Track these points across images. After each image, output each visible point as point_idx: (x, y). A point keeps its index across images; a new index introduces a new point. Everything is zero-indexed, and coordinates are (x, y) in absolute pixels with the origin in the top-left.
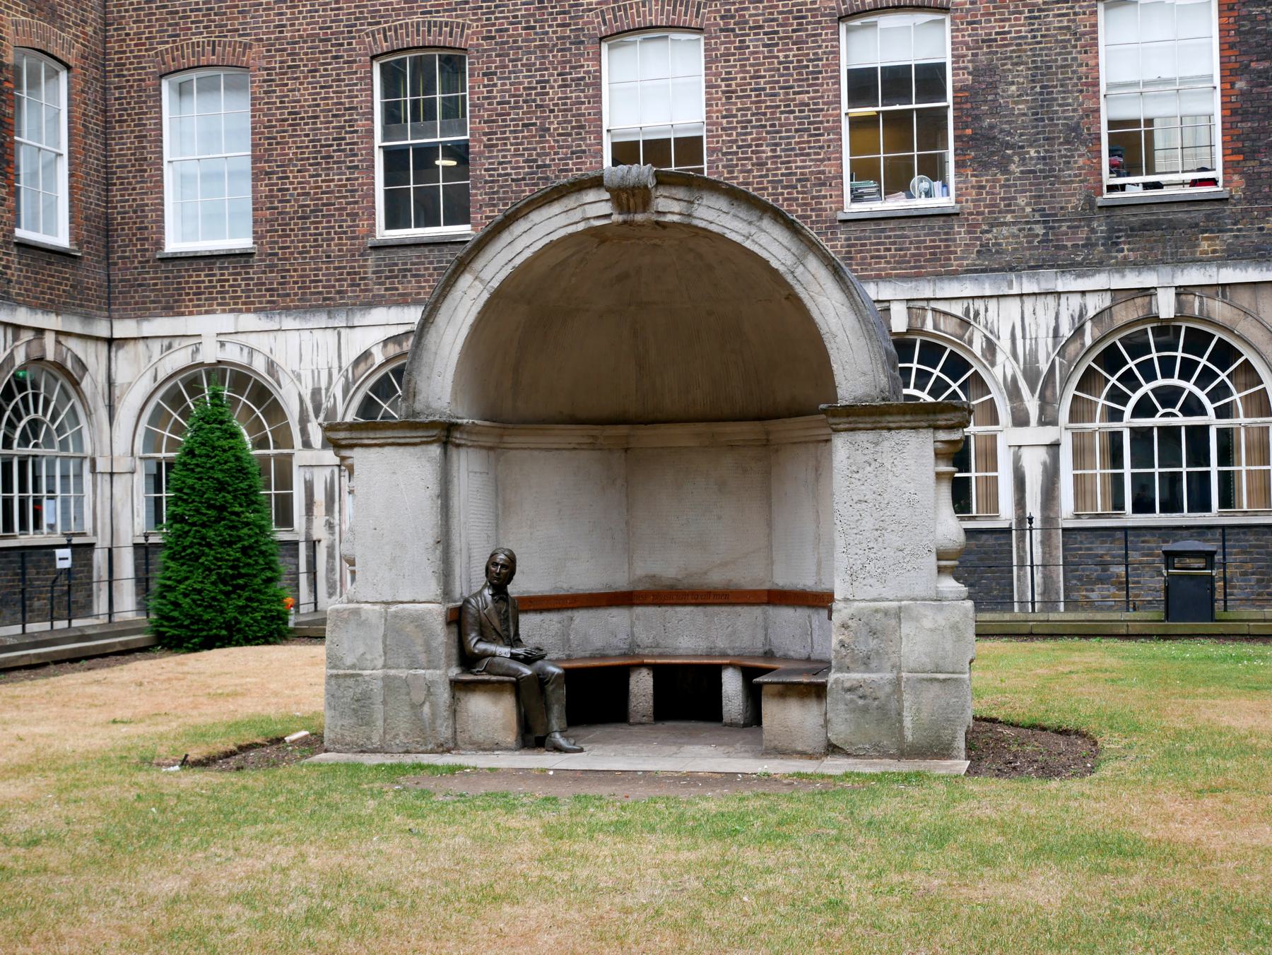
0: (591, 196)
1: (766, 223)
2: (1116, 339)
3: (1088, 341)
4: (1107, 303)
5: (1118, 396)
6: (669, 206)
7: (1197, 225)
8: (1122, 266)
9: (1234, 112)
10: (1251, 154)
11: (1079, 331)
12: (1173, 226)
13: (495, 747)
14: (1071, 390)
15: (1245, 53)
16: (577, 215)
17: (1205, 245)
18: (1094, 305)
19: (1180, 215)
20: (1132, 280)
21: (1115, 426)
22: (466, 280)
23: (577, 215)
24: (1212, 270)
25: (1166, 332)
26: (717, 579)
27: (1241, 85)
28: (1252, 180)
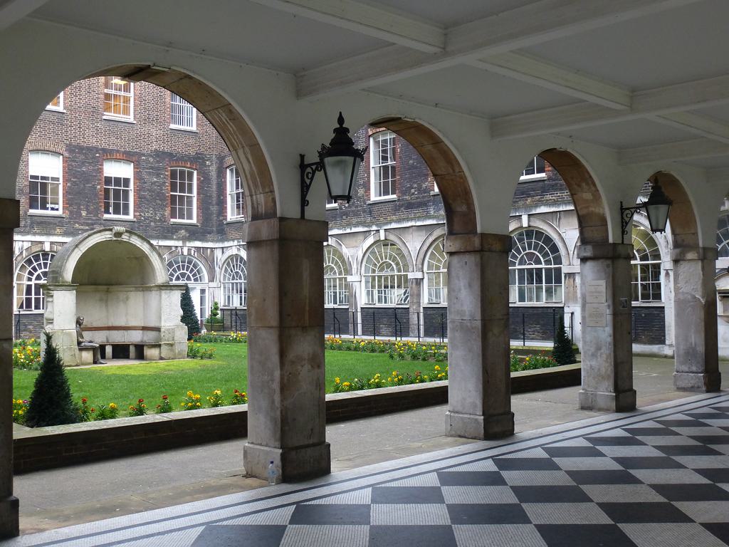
0: (107, 232)
1: (145, 243)
2: (31, 256)
3: (24, 256)
4: (30, 245)
5: (30, 273)
6: (125, 237)
7: (55, 224)
8: (35, 234)
9: (67, 192)
10: (71, 205)
11: (21, 253)
12: (50, 223)
13: (89, 364)
14: (17, 271)
15: (71, 175)
16: (103, 237)
17: (58, 230)
18: (26, 245)
19: (51, 220)
20: (38, 238)
21: (29, 283)
22: (76, 250)
23: (103, 237)
24: (60, 237)
25: (45, 255)
26: (95, 325)
27: (69, 184)
28: (71, 212)
